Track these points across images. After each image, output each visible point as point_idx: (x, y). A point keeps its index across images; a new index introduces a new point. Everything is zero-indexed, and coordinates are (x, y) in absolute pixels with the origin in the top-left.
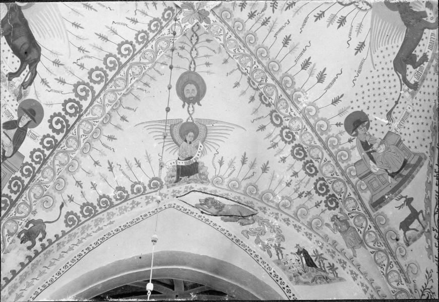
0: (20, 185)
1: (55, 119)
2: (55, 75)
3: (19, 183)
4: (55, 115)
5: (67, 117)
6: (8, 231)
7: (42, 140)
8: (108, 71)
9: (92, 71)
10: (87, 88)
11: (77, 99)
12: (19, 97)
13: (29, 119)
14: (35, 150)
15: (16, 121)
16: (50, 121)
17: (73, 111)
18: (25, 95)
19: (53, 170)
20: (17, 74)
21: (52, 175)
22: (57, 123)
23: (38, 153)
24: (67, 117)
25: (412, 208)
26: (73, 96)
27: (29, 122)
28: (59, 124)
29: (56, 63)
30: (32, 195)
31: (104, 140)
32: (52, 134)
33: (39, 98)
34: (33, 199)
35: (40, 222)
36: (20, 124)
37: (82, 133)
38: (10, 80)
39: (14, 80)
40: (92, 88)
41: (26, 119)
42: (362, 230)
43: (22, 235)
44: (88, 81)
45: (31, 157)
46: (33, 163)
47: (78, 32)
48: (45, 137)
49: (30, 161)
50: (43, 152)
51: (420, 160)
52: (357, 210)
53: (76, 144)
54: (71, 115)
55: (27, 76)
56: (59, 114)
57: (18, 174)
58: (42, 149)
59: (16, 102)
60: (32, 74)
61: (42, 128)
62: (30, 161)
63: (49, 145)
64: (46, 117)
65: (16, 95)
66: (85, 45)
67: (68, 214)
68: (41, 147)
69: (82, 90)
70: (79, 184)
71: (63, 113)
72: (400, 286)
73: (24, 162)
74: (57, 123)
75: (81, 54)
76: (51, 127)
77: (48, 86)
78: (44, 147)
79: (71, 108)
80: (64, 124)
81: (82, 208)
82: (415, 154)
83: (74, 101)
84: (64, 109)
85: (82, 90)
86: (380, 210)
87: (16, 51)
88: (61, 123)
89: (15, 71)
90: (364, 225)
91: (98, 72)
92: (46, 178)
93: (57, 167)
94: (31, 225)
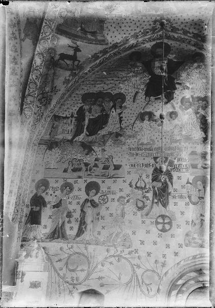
25: (75, 53)
42: (44, 35)
51: (104, 41)
52: (51, 23)
72: (36, 81)
82: (104, 36)
86: (59, 36)
90: (47, 34)
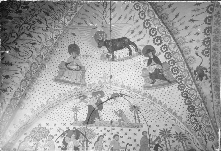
0: (176, 69)
1: (155, 41)
2: (137, 34)
3: (175, 69)
4: (154, 41)
5: (156, 36)
6: (190, 85)
7: (162, 51)
8: (141, 10)
9: (140, 17)
10: (146, 22)
11: (150, 28)
12: (140, 53)
13: (151, 53)
14: (165, 56)
15: (149, 59)
16: (155, 44)
17: (155, 32)
18: (140, 50)
19: (175, 52)
20: (131, 51)
21: (177, 54)
22: (157, 41)
23: (167, 55)
24: (156, 36)
26: (148, 30)
27: (152, 53)
28: (158, 40)
29: (133, 32)
30: (181, 67)
31: (176, 20)
32: (161, 46)
33: (144, 45)
34: (183, 67)
35: (198, 68)
36: (151, 57)
37: (164, 33)
38: (131, 55)
39: (132, 53)
40: (147, 20)
41: (151, 55)
43: (199, 79)
44: (144, 20)
45: (167, 59)
46: (170, 59)
47: (123, 17)
48: (161, 49)
49: (168, 60)
50: (167, 53)
53: (168, 37)
54: (156, 34)
55: (133, 47)
56: (154, 39)
57: (171, 67)
58: (166, 53)
59: (141, 56)
60: (133, 44)
61: (157, 49)
62: (168, 60)
63: (165, 49)
64: (153, 45)
65: (139, 55)
66: (129, 16)
67: (203, 53)
68: (165, 53)
69: (147, 25)
70: (191, 41)
71: (154, 37)
73: (168, 63)
74: (157, 41)
75: (132, 19)
76: (158, 45)
77: (141, 39)
78: (165, 51)
79: (153, 33)
80: (159, 38)
81: (204, 44)
83: (150, 30)
84: (153, 36)
85: (147, 25)
87: (121, 48)
88: (158, 39)
89: (129, 51)
91: (141, 14)
92: (177, 57)
93: (175, 50)
94: (197, 73)
